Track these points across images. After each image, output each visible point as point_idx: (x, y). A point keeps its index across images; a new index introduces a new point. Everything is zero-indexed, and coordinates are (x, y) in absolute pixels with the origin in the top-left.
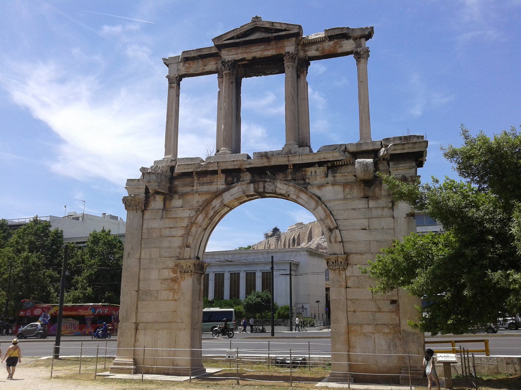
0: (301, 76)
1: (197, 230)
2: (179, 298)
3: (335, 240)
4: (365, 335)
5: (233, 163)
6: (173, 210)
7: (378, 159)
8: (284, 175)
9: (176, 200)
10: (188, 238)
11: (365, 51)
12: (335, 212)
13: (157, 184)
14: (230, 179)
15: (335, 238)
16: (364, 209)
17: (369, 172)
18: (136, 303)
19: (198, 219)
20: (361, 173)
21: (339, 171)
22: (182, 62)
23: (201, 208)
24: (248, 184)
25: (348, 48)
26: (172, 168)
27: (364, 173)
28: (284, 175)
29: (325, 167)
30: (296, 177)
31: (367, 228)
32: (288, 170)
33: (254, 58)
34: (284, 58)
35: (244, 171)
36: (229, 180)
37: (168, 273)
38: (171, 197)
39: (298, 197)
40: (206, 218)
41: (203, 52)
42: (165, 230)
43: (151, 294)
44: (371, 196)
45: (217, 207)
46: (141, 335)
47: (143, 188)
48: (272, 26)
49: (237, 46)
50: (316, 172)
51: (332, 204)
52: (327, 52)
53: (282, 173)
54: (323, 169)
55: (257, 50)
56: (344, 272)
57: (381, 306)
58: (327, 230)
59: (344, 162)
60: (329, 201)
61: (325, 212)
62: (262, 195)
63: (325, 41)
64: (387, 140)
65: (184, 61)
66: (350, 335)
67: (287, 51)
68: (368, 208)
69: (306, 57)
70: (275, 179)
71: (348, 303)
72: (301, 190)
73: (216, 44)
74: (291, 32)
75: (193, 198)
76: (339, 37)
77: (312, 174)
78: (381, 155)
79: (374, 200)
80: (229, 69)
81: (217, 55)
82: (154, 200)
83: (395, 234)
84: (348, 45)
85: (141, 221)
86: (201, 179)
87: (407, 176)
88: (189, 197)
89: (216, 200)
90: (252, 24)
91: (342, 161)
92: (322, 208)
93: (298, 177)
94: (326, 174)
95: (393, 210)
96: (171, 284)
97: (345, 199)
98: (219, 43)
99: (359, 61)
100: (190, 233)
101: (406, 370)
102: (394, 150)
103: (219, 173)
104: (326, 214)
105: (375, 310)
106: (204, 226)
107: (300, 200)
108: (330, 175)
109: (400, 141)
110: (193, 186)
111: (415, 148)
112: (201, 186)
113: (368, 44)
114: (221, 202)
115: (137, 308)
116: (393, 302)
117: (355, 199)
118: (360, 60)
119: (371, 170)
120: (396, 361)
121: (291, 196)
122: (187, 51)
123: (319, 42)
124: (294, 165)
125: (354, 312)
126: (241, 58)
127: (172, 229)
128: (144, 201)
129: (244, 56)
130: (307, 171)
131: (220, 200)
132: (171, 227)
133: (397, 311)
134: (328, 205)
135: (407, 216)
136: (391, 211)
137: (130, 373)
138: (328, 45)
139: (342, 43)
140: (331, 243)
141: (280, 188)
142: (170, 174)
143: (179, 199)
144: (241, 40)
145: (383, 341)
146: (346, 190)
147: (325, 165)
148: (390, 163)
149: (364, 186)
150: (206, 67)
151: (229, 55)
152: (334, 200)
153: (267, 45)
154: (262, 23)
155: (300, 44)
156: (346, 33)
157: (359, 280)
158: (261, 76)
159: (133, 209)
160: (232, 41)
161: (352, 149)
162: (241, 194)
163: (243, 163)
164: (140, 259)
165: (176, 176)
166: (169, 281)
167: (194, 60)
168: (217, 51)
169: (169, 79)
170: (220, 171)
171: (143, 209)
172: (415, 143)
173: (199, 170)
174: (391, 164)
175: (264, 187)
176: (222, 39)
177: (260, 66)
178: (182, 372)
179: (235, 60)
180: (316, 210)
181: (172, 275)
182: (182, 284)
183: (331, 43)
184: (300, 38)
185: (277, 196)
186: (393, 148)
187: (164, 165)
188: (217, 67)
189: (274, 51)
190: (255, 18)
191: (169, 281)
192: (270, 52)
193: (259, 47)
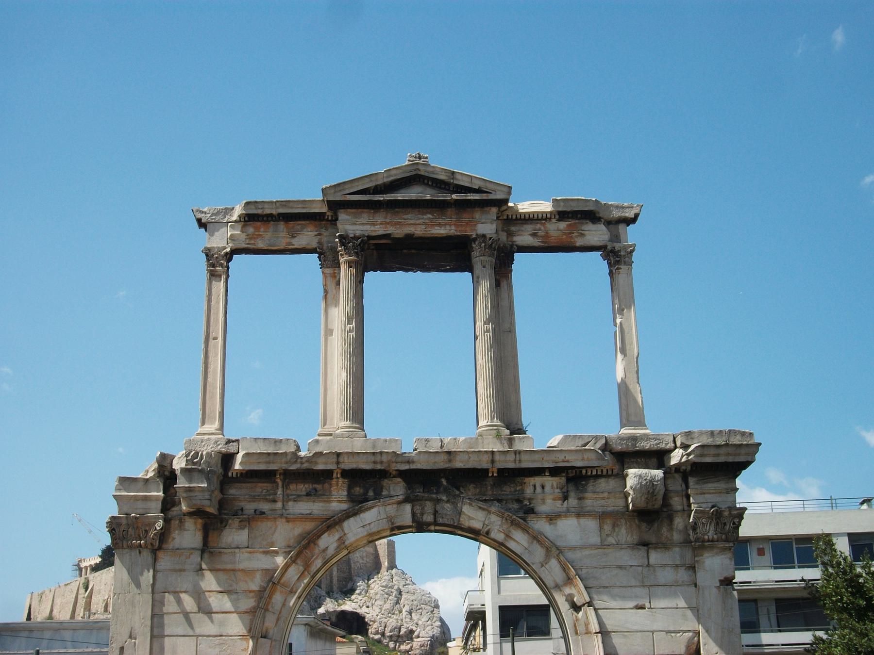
0: (501, 282)
1: (285, 600)
6: (226, 553)
7: (668, 470)
8: (478, 490)
9: (234, 530)
10: (264, 617)
12: (584, 571)
14: (358, 490)
15: (587, 625)
16: (640, 569)
17: (655, 495)
19: (286, 575)
20: (642, 496)
21: (590, 487)
22: (240, 221)
24: (399, 503)
25: (596, 239)
26: (227, 459)
27: (647, 498)
28: (478, 490)
29: (563, 478)
30: (503, 495)
31: (647, 605)
33: (409, 237)
34: (474, 246)
35: (392, 476)
36: (357, 493)
38: (221, 523)
39: (508, 536)
40: (307, 573)
41: (292, 208)
44: (654, 542)
45: (331, 551)
48: (453, 179)
49: (373, 209)
50: (543, 487)
52: (553, 241)
53: (472, 485)
54: (561, 480)
58: (569, 607)
59: (602, 471)
60: (573, 549)
62: (420, 527)
63: (550, 218)
64: (688, 434)
65: (245, 221)
68: (648, 565)
69: (512, 246)
70: (459, 496)
72: (513, 523)
73: (331, 198)
74: (491, 197)
75: (273, 528)
76: (579, 216)
77: (536, 491)
78: (672, 463)
79: (658, 550)
80: (357, 254)
81: (322, 217)
82: (181, 526)
84: (596, 234)
86: (292, 487)
87: (720, 506)
88: (264, 526)
89: (329, 535)
90: (410, 168)
91: (597, 468)
92: (560, 562)
93: (507, 495)
94: (565, 492)
95: (695, 572)
97: (603, 545)
98: (338, 197)
99: (618, 269)
100: (270, 607)
102: (702, 455)
103: (335, 476)
107: (512, 545)
108: (572, 494)
109: (711, 439)
110: (275, 501)
111: (739, 455)
113: (632, 235)
114: (338, 539)
117: (624, 546)
118: (620, 266)
119: (661, 493)
121: (493, 535)
122: (256, 202)
123: (538, 219)
124: (501, 471)
126: (381, 232)
128: (161, 529)
129: (391, 230)
130: (525, 483)
131: (337, 536)
134: (570, 555)
136: (691, 572)
138: (556, 229)
139: (583, 228)
141: (469, 517)
142: (221, 471)
143: (241, 528)
146: (605, 527)
147: (564, 474)
152: (582, 547)
153: (438, 215)
154: (431, 169)
155: (501, 218)
156: (592, 210)
158: (416, 272)
159: (131, 547)
161: (617, 448)
162: (385, 525)
165: (234, 476)
167: (268, 221)
168: (324, 209)
169: (207, 255)
170: (340, 471)
171: (156, 547)
172: (740, 446)
173: (294, 467)
175: (435, 513)
176: (344, 190)
177: (413, 251)
180: (547, 566)
183: (563, 225)
184: (504, 207)
186: (698, 452)
187: (209, 450)
188: (320, 243)
189: (453, 228)
190: (416, 157)
192: (444, 228)
193: (422, 217)
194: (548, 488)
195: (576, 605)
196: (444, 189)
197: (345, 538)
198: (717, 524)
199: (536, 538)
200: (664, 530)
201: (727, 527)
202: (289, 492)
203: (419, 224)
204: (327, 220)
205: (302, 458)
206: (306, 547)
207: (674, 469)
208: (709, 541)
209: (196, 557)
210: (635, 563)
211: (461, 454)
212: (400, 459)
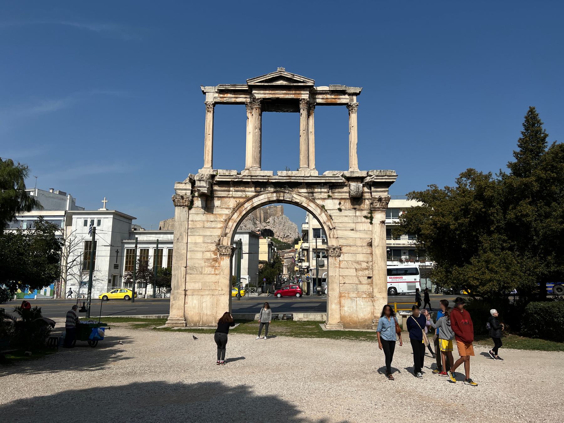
2: (220, 273)
3: (333, 236)
4: (351, 299)
5: (263, 178)
7: (365, 184)
11: (356, 105)
13: (206, 189)
14: (258, 189)
16: (353, 217)
18: (185, 276)
23: (236, 209)
31: (355, 229)
34: (300, 102)
37: (210, 255)
41: (236, 87)
42: (207, 223)
45: (248, 209)
46: (189, 299)
49: (265, 88)
51: (332, 212)
52: (329, 101)
61: (327, 216)
66: (341, 298)
67: (303, 98)
68: (356, 216)
96: (213, 263)
104: (328, 218)
110: (229, 191)
112: (235, 192)
115: (186, 280)
116: (369, 278)
120: (370, 315)
126: (267, 97)
127: (213, 222)
129: (271, 96)
132: (212, 220)
133: (371, 284)
143: (219, 200)
144: (269, 84)
145: (361, 302)
149: (353, 201)
150: (238, 99)
151: (259, 95)
160: (262, 84)
164: (187, 243)
166: (211, 261)
174: (372, 188)
177: (279, 105)
179: (263, 99)
186: (376, 177)
189: (293, 96)
192: (290, 95)
193: (282, 91)
195: (330, 228)
196: (290, 81)
197: (253, 204)
201: (384, 204)
203: (281, 94)
204: (249, 92)
206: (240, 207)
208: (377, 208)
210: (350, 215)
212: (273, 178)
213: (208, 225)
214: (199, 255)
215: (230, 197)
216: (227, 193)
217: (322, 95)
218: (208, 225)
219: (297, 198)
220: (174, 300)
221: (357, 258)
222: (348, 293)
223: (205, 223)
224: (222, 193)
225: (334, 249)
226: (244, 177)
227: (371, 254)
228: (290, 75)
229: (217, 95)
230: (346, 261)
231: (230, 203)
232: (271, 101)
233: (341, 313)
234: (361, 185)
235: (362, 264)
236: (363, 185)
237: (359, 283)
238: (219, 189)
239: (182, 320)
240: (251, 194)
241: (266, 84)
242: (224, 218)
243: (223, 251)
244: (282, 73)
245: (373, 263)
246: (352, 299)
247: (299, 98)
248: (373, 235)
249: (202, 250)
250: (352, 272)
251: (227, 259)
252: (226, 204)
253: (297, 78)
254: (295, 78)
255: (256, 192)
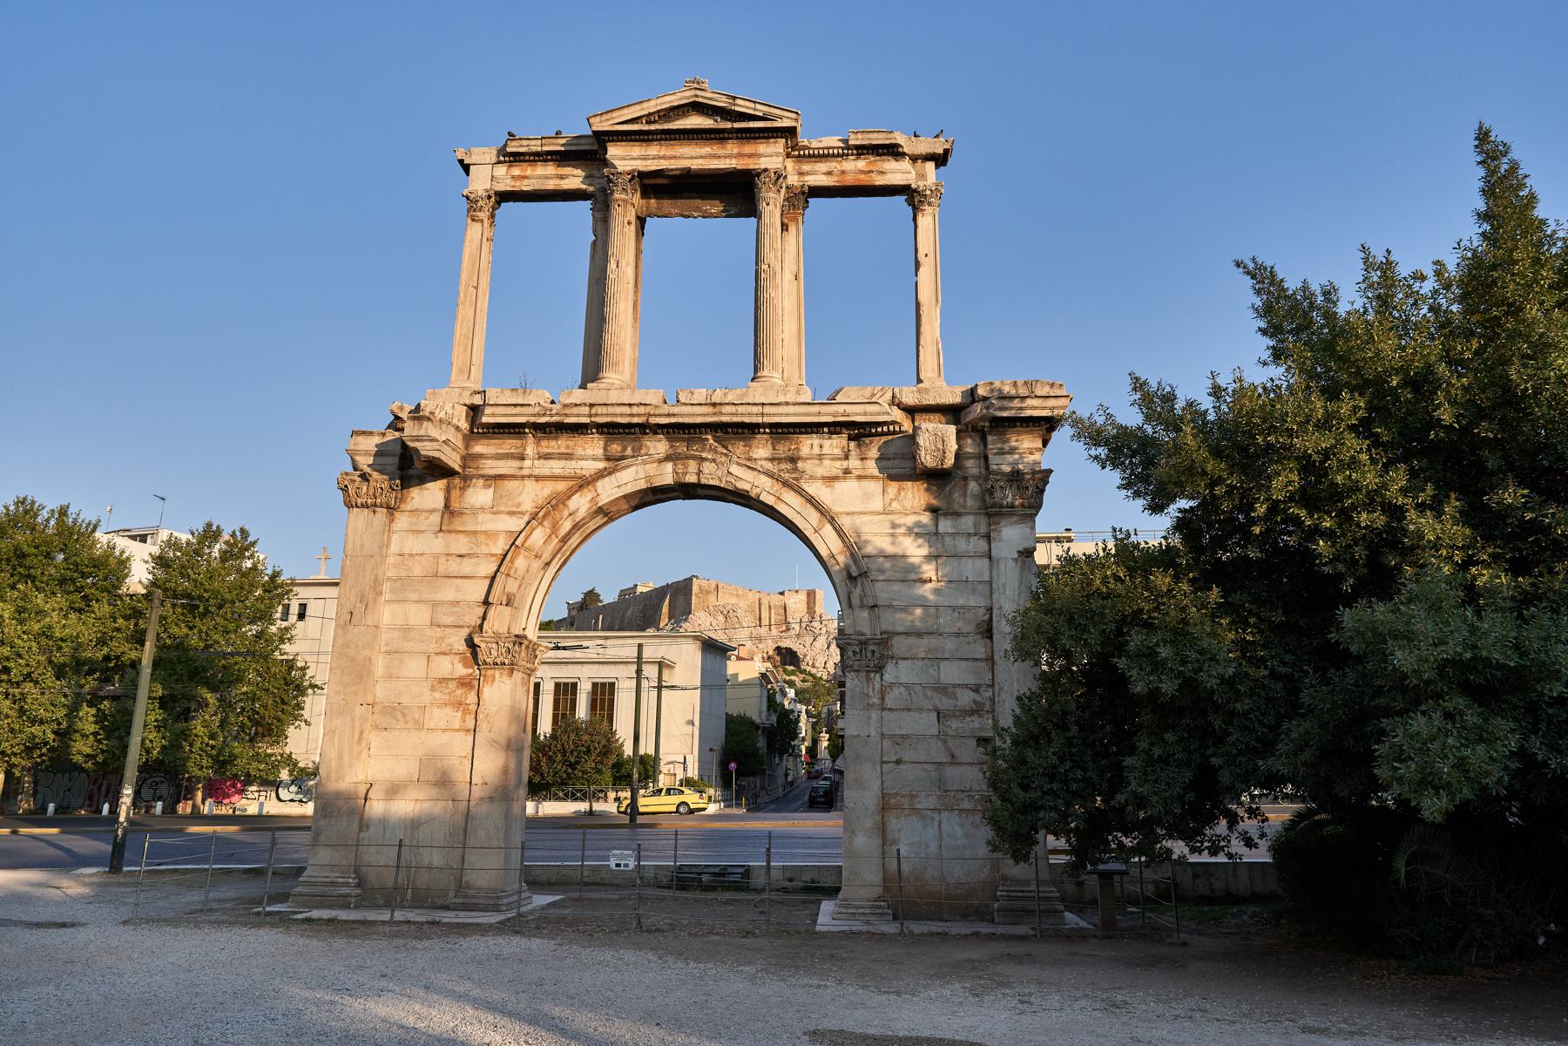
3: (861, 602)
5: (627, 410)
14: (615, 448)
22: (505, 162)
23: (541, 514)
24: (660, 461)
25: (899, 178)
32: (759, 436)
37: (450, 666)
43: (404, 716)
45: (582, 514)
47: (394, 455)
48: (735, 105)
50: (821, 447)
52: (849, 180)
55: (694, 154)
56: (878, 675)
57: (956, 752)
61: (840, 536)
67: (763, 167)
68: (937, 533)
69: (803, 186)
70: (726, 455)
71: (884, 744)
72: (785, 484)
73: (595, 129)
78: (968, 419)
83: (992, 594)
85: (386, 537)
86: (544, 443)
88: (510, 485)
89: (581, 496)
92: (835, 528)
95: (990, 543)
96: (459, 692)
100: (512, 572)
101: (1006, 891)
105: (944, 760)
106: (546, 557)
110: (523, 459)
112: (542, 461)
123: (833, 156)
125: (898, 762)
127: (465, 559)
131: (590, 496)
132: (461, 553)
135: (1020, 556)
136: (983, 544)
137: (346, 906)
140: (851, 610)
143: (487, 487)
145: (957, 828)
148: (990, 438)
150: (566, 181)
151: (624, 158)
157: (910, 694)
163: (652, 412)
166: (452, 685)
175: (699, 472)
178: (482, 901)
181: (461, 671)
182: (487, 691)
183: (861, 164)
185: (726, 495)
189: (734, 161)
191: (452, 685)
194: (826, 450)
198: (1018, 488)
199: (811, 500)
200: (956, 495)
202: (540, 449)
203: (696, 158)
204: (600, 160)
205: (551, 410)
206: (554, 508)
207: (970, 427)
209: (436, 518)
211: (727, 407)
212: (657, 412)
213: (454, 566)
214: (414, 667)
215: (523, 477)
216: (516, 463)
217: (828, 164)
218: (454, 566)
219: (746, 480)
220: (325, 816)
221: (942, 675)
222: (912, 796)
223: (442, 560)
224: (500, 463)
225: (863, 644)
226: (567, 411)
227: (990, 660)
228: (724, 98)
229: (501, 170)
230: (907, 686)
231: (523, 495)
232: (665, 181)
233: (887, 866)
234: (952, 429)
235: (959, 695)
236: (958, 432)
237: (949, 760)
238: (490, 452)
239: (347, 884)
240: (589, 464)
241: (646, 127)
242: (499, 546)
243: (494, 653)
244: (698, 93)
245: (996, 687)
246: (923, 818)
247: (751, 167)
248: (994, 596)
249: (423, 647)
250: (925, 723)
251: (505, 678)
252: (509, 500)
253: (742, 107)
254: (737, 109)
255: (608, 459)
